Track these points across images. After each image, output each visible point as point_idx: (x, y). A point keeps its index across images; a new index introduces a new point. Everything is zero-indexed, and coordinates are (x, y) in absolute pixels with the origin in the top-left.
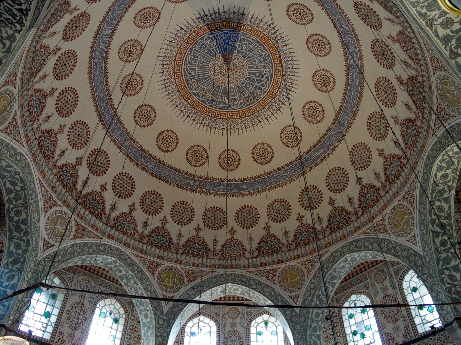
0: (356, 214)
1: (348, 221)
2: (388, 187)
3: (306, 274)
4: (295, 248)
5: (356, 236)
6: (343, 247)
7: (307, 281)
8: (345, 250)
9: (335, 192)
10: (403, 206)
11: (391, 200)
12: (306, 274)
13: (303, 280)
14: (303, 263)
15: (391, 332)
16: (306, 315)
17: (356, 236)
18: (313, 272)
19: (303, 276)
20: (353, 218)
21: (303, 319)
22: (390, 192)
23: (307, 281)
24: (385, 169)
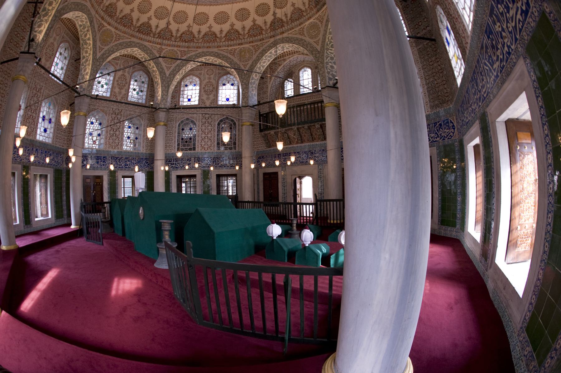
0: (154, 35)
1: (148, 34)
2: (178, 40)
3: (113, 41)
4: (119, 23)
5: (147, 44)
6: (138, 43)
7: (112, 44)
8: (138, 45)
9: (156, 17)
10: (177, 53)
11: (174, 46)
12: (113, 41)
13: (110, 43)
14: (116, 34)
15: (117, 92)
16: (101, 63)
17: (147, 44)
18: (116, 43)
19: (112, 40)
20: (152, 35)
21: (98, 63)
22: (176, 43)
23: (112, 44)
24: (183, 33)
